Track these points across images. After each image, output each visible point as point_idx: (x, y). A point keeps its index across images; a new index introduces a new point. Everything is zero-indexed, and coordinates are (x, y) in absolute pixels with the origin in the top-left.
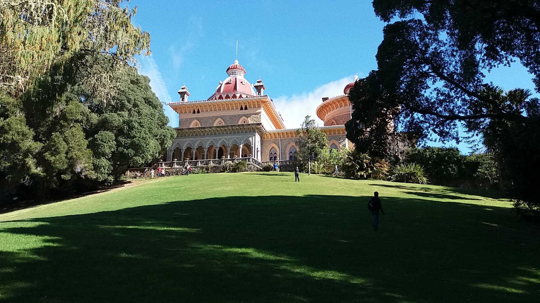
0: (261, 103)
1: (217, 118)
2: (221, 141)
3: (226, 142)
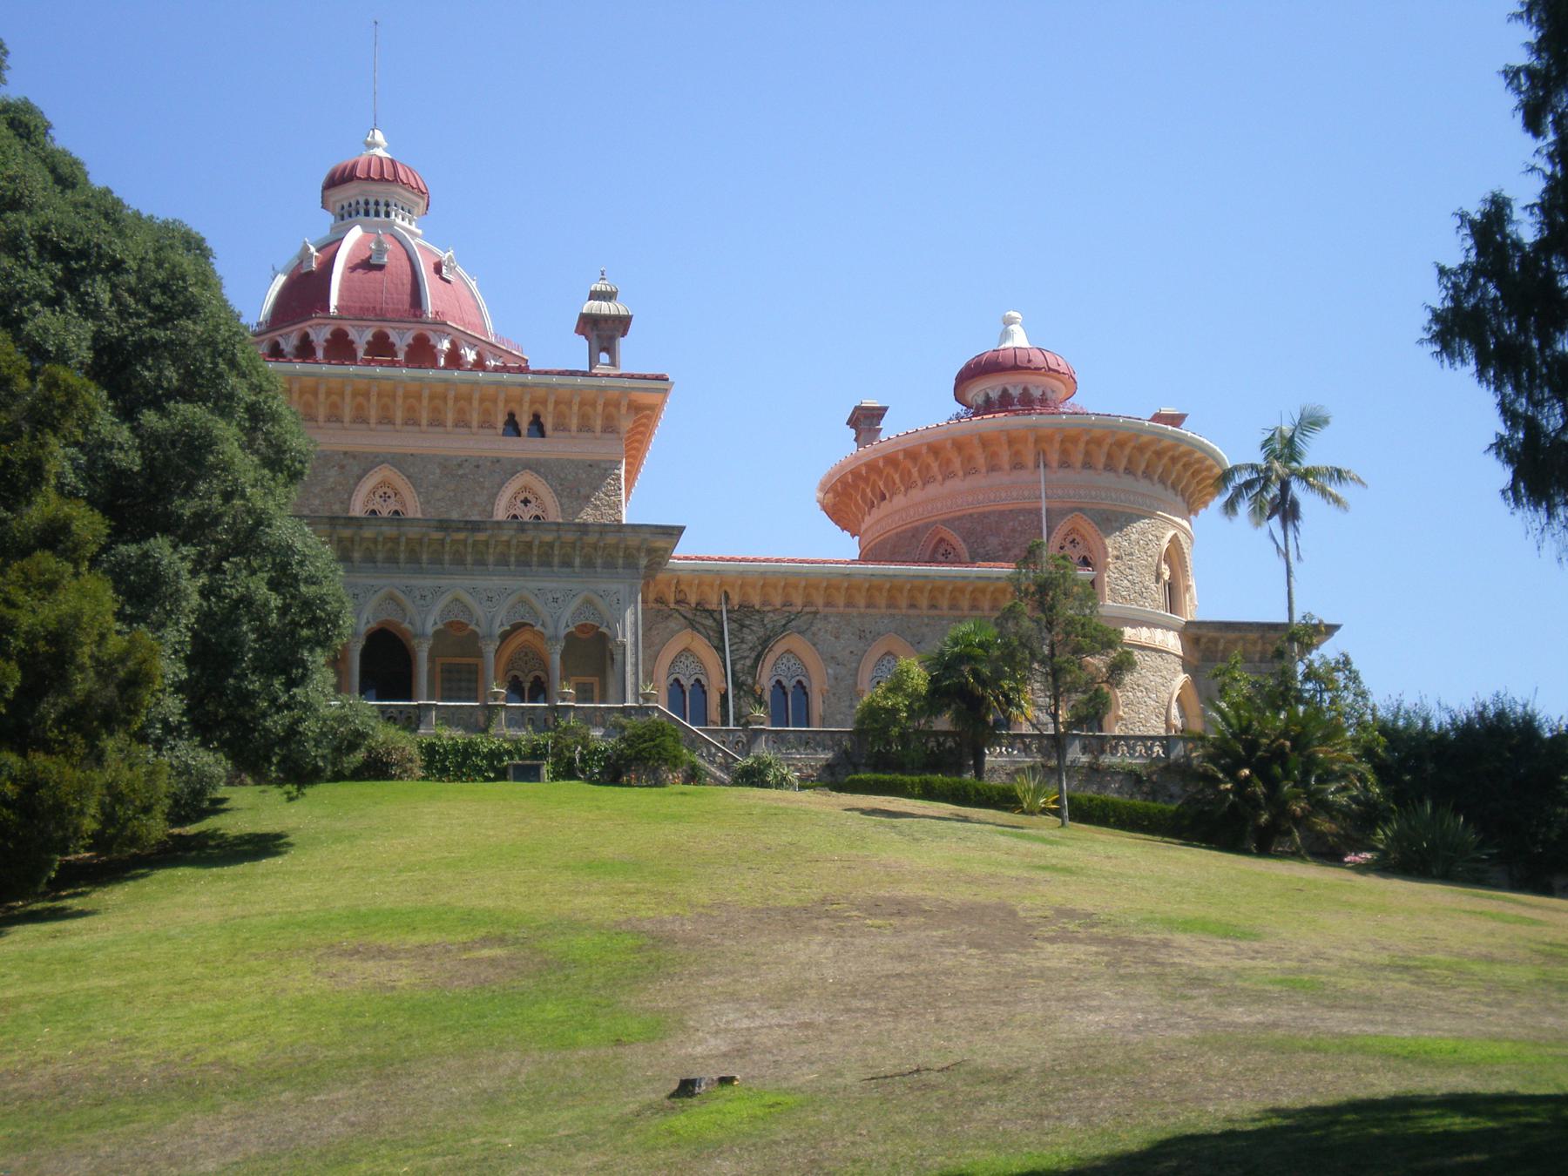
0: (624, 410)
1: (370, 462)
2: (447, 598)
3: (479, 611)
